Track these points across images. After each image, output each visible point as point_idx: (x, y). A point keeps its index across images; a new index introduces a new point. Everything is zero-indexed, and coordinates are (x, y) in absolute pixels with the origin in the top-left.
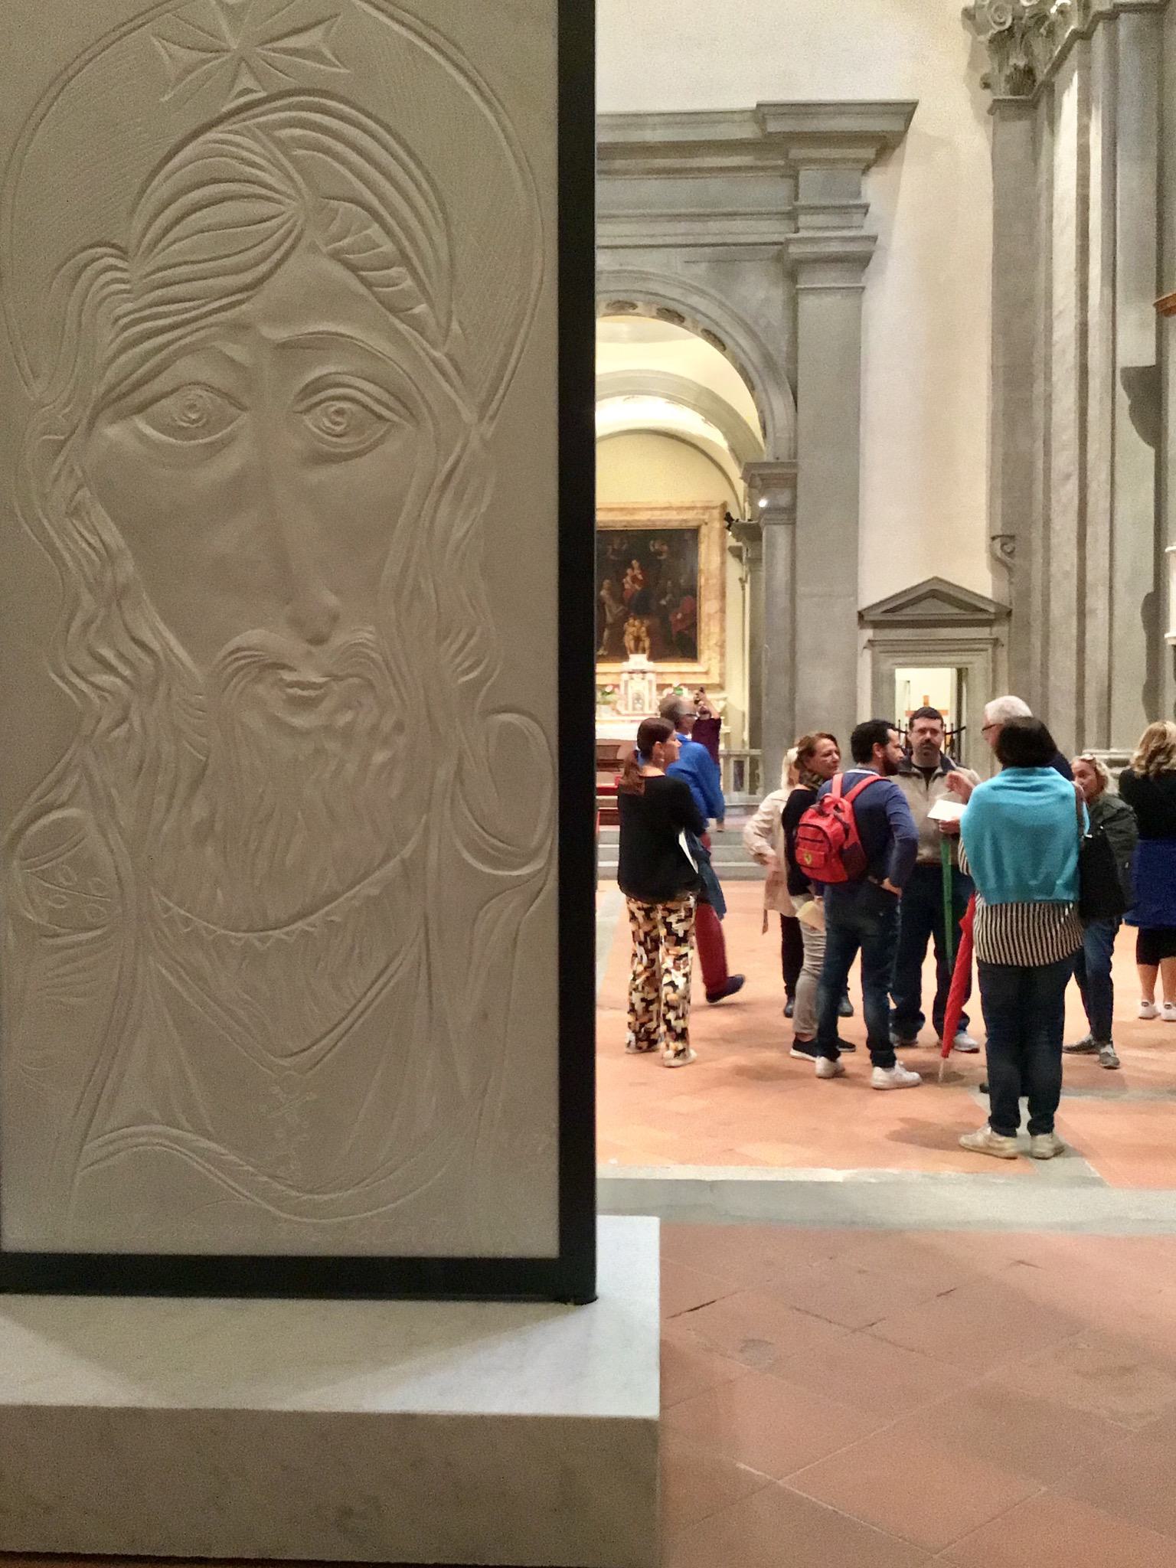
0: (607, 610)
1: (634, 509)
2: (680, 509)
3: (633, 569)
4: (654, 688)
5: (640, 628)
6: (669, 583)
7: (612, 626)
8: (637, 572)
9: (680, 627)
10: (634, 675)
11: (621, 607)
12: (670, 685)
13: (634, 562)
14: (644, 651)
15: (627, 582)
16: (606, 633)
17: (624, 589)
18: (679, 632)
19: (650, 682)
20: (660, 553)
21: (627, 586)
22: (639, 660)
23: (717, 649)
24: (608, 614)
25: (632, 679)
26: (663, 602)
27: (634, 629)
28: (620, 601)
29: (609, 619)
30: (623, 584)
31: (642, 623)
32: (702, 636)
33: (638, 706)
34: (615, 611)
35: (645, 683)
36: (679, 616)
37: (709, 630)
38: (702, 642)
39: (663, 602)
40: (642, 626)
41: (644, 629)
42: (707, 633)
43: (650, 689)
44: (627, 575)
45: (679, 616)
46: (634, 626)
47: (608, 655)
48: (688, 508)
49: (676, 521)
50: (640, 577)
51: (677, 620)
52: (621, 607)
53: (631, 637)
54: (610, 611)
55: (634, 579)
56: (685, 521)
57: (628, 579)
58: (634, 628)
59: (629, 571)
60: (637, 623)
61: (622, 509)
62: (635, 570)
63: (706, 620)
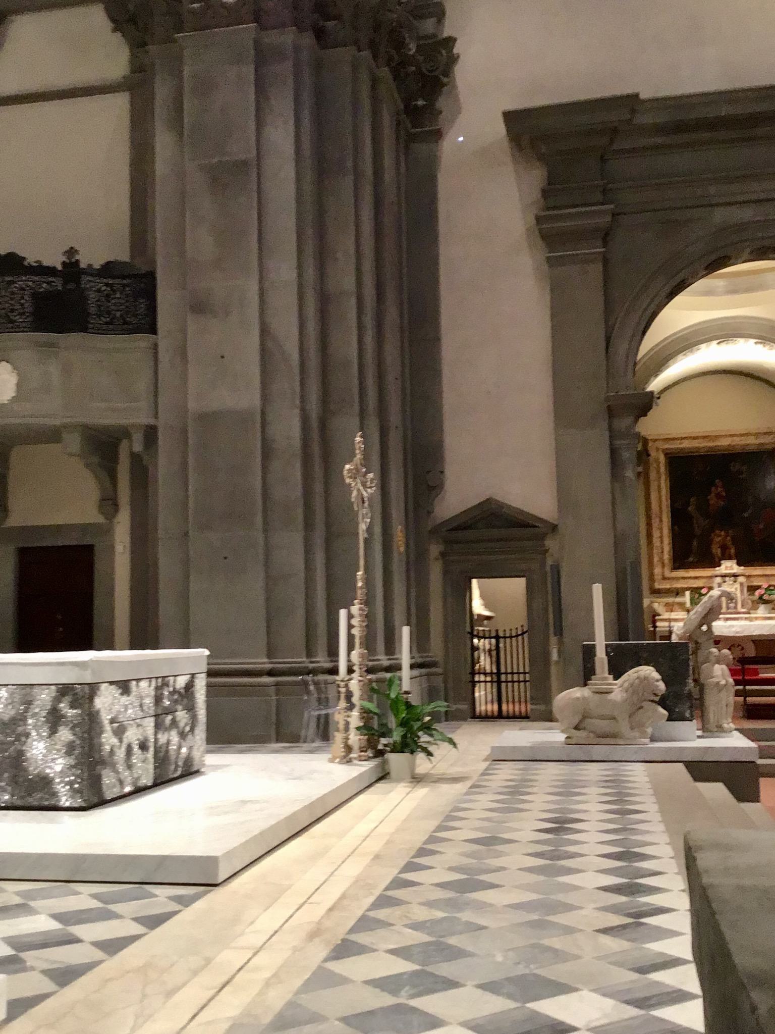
1: (716, 436)
2: (757, 435)
4: (745, 589)
10: (727, 579)
11: (707, 522)
12: (759, 587)
16: (695, 543)
19: (741, 584)
21: (712, 502)
22: (729, 566)
25: (725, 582)
26: (746, 515)
29: (698, 531)
30: (708, 500)
33: (732, 605)
35: (737, 586)
39: (746, 515)
43: (742, 591)
44: (710, 493)
45: (761, 526)
46: (720, 536)
48: (765, 434)
49: (752, 445)
50: (724, 494)
52: (707, 522)
55: (718, 496)
56: (762, 444)
57: (713, 495)
58: (719, 538)
60: (723, 533)
61: (704, 437)
62: (719, 488)
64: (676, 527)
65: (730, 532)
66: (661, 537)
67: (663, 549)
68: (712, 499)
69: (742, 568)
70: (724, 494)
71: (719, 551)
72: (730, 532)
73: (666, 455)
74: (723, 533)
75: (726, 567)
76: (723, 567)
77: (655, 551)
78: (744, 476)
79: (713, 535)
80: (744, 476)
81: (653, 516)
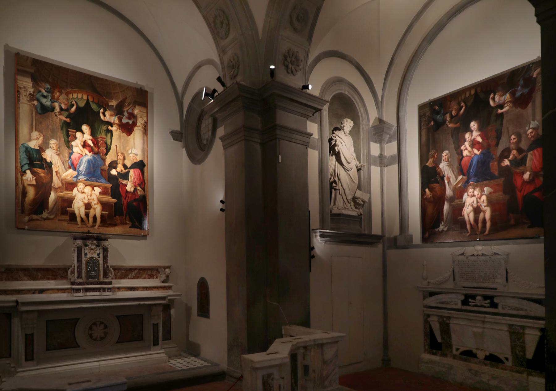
0: (446, 181)
3: (472, 131)
5: (480, 198)
6: (513, 137)
7: (451, 200)
9: (528, 189)
15: (466, 149)
16: (446, 207)
17: (463, 157)
20: (501, 106)
21: (465, 153)
26: (506, 162)
27: (474, 198)
28: (461, 171)
29: (449, 192)
31: (482, 191)
34: (454, 182)
36: (527, 176)
39: (506, 162)
40: (482, 195)
41: (484, 198)
44: (465, 140)
45: (527, 176)
46: (474, 196)
47: (448, 230)
50: (479, 139)
51: (524, 180)
52: (460, 177)
53: (471, 208)
55: (474, 144)
57: (467, 144)
60: (477, 192)
64: (427, 190)
65: (486, 189)
68: (467, 150)
72: (486, 189)
74: (477, 192)
78: (506, 109)
79: (465, 195)
80: (506, 109)
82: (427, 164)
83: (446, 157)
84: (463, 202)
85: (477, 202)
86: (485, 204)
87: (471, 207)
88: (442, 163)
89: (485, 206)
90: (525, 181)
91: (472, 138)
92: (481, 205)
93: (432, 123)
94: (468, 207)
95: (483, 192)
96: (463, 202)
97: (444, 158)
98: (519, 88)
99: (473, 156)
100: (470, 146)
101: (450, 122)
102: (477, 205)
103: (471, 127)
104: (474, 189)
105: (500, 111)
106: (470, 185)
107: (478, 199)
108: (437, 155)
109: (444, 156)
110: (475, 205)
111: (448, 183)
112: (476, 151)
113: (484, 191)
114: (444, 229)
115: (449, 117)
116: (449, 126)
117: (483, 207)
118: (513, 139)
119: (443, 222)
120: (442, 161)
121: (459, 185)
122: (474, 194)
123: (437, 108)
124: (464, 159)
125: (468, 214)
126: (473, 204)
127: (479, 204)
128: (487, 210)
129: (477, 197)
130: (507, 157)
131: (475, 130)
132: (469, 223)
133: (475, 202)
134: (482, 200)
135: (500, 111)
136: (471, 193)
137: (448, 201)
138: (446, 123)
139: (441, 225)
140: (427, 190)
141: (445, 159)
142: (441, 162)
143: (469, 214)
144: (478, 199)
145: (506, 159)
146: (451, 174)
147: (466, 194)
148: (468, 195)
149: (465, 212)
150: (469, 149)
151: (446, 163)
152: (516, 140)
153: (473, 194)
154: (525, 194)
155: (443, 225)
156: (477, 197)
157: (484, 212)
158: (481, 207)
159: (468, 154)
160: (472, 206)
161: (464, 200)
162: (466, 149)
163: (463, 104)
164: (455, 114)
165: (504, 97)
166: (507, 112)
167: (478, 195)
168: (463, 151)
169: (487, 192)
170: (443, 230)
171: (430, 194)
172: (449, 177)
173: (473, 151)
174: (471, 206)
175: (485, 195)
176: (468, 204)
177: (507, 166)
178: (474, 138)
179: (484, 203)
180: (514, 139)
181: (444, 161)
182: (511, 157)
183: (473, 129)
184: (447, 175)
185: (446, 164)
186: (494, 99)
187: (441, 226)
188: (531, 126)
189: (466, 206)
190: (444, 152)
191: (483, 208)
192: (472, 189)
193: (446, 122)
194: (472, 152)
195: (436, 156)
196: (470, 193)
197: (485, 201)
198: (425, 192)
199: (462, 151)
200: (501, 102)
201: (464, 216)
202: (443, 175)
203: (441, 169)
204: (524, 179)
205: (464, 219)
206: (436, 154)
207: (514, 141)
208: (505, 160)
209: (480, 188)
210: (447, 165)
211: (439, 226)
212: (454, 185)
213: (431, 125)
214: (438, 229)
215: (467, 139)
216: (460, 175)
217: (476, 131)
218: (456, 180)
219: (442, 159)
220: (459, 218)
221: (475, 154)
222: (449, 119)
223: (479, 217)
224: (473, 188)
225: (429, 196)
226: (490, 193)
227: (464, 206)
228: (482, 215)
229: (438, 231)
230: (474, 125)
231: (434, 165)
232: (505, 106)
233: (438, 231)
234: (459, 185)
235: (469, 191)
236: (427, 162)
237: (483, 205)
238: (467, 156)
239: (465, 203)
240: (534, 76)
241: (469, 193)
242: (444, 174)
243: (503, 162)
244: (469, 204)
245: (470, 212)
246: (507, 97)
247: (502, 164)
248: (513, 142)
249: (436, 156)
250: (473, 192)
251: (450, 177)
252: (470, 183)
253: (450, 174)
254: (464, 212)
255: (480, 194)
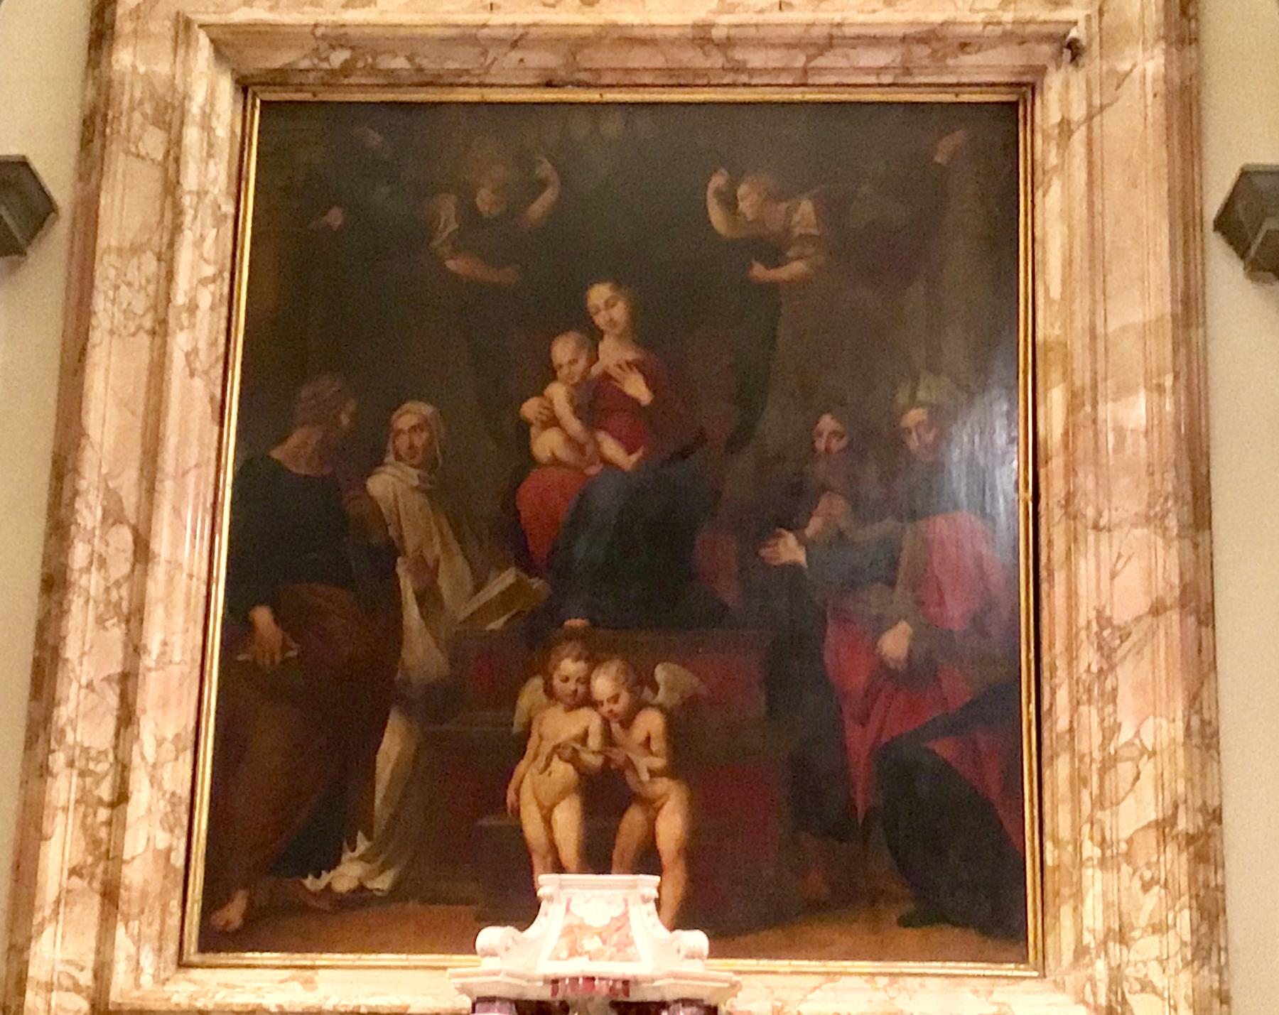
3: (594, 335)
5: (627, 722)
6: (827, 423)
8: (613, 353)
13: (599, 294)
14: (647, 861)
15: (553, 421)
17: (532, 461)
18: (884, 754)
21: (547, 444)
23: (1176, 862)
24: (412, 613)
26: (790, 550)
27: (589, 720)
32: (1060, 771)
37: (1110, 731)
38: (1061, 820)
39: (790, 550)
40: (637, 707)
41: (651, 723)
42: (1090, 741)
44: (550, 373)
46: (588, 701)
47: (397, 893)
50: (637, 388)
53: (562, 771)
54: (429, 597)
57: (558, 393)
59: (564, 350)
60: (603, 685)
63: (1089, 657)
64: (263, 616)
65: (660, 673)
66: (127, 681)
67: (123, 769)
69: (697, 939)
70: (637, 388)
71: (568, 820)
73: (244, 86)
74: (603, 685)
75: (574, 934)
76: (549, 922)
77: (63, 788)
78: (796, 268)
79: (532, 692)
80: (796, 268)
81: (88, 514)
82: (276, 454)
83: (420, 440)
84: (516, 729)
85: (608, 738)
86: (659, 763)
87: (570, 767)
88: (389, 469)
89: (653, 773)
90: (889, 669)
91: (596, 370)
92: (629, 763)
93: (335, 217)
94: (548, 765)
95: (647, 692)
96: (516, 729)
97: (403, 442)
98: (865, 189)
99: (593, 470)
100: (577, 411)
101: (459, 245)
102: (607, 761)
103: (593, 310)
104: (594, 661)
105: (759, 271)
106: (572, 635)
107: (615, 727)
108: (353, 416)
109: (400, 432)
110: (595, 761)
111: (421, 599)
112: (612, 448)
113: (655, 688)
114: (369, 885)
115: (452, 219)
116: (451, 264)
117: (645, 777)
118: (825, 434)
119: (369, 836)
120: (390, 458)
121: (491, 621)
122: (589, 692)
123: (375, 139)
124: (535, 472)
125: (547, 804)
126: (578, 746)
127: (618, 756)
128: (664, 797)
129: (605, 709)
130: (795, 527)
131: (617, 331)
132: (549, 859)
133: (594, 742)
134: (639, 732)
135: (759, 271)
136: (571, 686)
137: (407, 712)
138: (435, 244)
139: (347, 855)
140: (263, 616)
141: (411, 447)
142: (382, 464)
143: (551, 810)
144: (615, 727)
145: (790, 530)
146: (444, 545)
147: (537, 683)
148: (549, 691)
149: (523, 790)
150: (575, 426)
151: (414, 472)
152: (844, 442)
153: (581, 689)
154: (884, 740)
155: (361, 858)
156: (605, 709)
157: (652, 807)
158: (628, 773)
159: (563, 453)
160: (574, 760)
161: (524, 720)
162: (553, 421)
163: (545, 169)
164: (495, 212)
165: (783, 206)
166: (800, 283)
167: (615, 699)
168: (533, 430)
169: (670, 689)
170: (361, 888)
171: (285, 648)
172: (430, 563)
173: (598, 445)
174: (567, 761)
175: (661, 708)
176: (547, 748)
177: (795, 566)
178: (606, 376)
179: (652, 753)
180: (834, 433)
181: (398, 457)
182: (814, 526)
183: (600, 320)
184: (420, 548)
185: (416, 483)
186: (729, 201)
187: (351, 860)
188: (921, 395)
189: (536, 757)
190: (407, 406)
191: (640, 782)
192: (577, 659)
193: (431, 239)
194: (589, 449)
195: (345, 420)
196: (566, 680)
197: (656, 745)
198: (250, 626)
199: (523, 429)
200: (775, 226)
201: (517, 812)
202: (390, 540)
203: (371, 498)
204: (879, 654)
205: (520, 830)
206: (351, 406)
207: (836, 445)
208: (780, 536)
209: (626, 660)
210: (417, 488)
211: (333, 863)
212: (463, 614)
213: (328, 227)
214: (326, 878)
215: (561, 366)
216: (501, 569)
217: (620, 337)
218: (478, 588)
219: (390, 447)
220: (485, 822)
221: (607, 463)
222: (453, 226)
223: (615, 832)
224: (586, 653)
225: (278, 658)
226: (691, 703)
227: (522, 755)
228: (634, 818)
229: (328, 887)
230: (609, 305)
231: (327, 470)
232: (790, 254)
233: (328, 887)
234: (497, 625)
235: (556, 667)
236: (282, 439)
237: (644, 763)
238: (555, 461)
239: (527, 734)
240: (939, 159)
241: (557, 682)
242: (392, 532)
243: (772, 542)
244: (556, 748)
245: (563, 795)
246: (802, 215)
247: (764, 552)
248: (827, 450)
249: (345, 420)
250: (587, 681)
251: (437, 561)
252: (567, 623)
253: (437, 549)
254: (518, 793)
255: (625, 698)
